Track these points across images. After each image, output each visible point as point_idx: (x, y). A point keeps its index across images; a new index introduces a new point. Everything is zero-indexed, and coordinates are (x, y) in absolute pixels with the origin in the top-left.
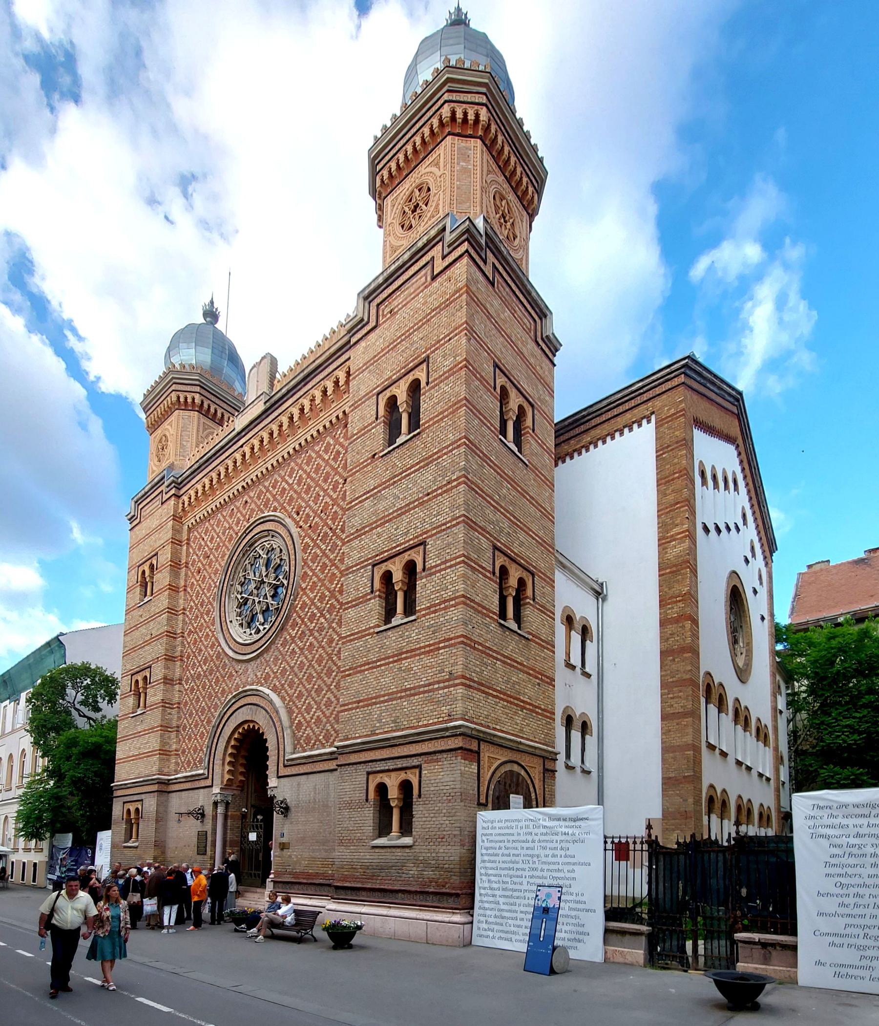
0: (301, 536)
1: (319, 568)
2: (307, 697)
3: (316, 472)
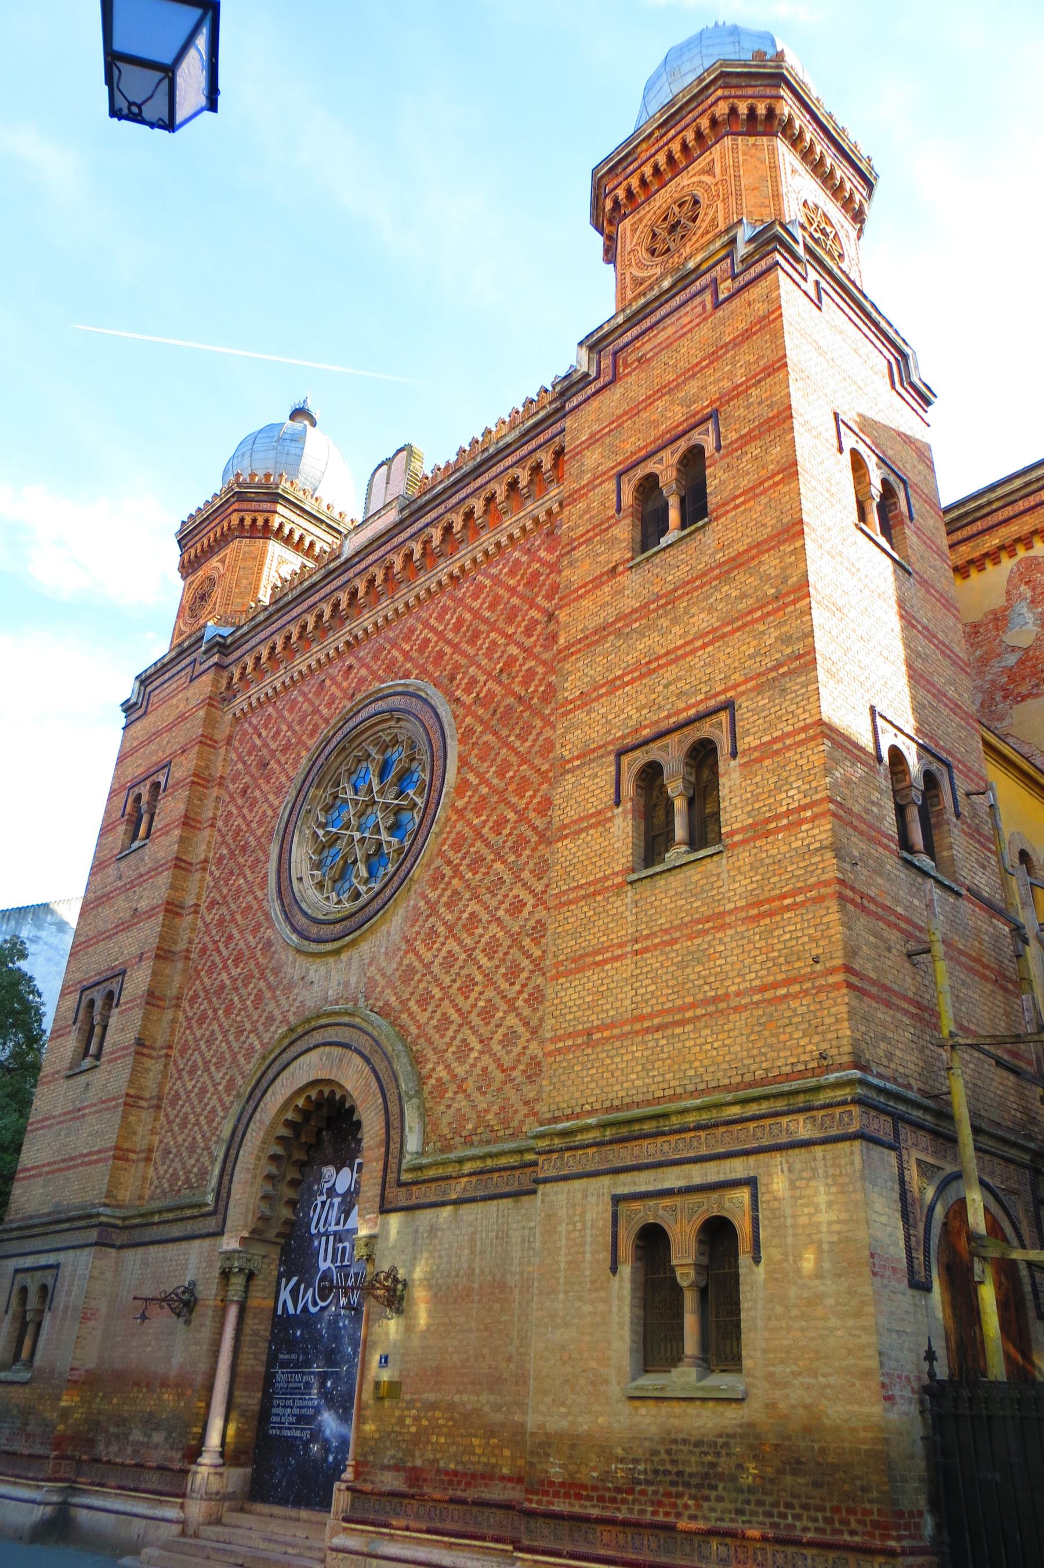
0: (456, 717)
1: (493, 769)
2: (461, 1026)
3: (492, 607)
